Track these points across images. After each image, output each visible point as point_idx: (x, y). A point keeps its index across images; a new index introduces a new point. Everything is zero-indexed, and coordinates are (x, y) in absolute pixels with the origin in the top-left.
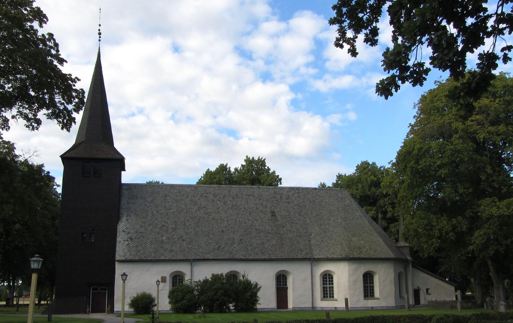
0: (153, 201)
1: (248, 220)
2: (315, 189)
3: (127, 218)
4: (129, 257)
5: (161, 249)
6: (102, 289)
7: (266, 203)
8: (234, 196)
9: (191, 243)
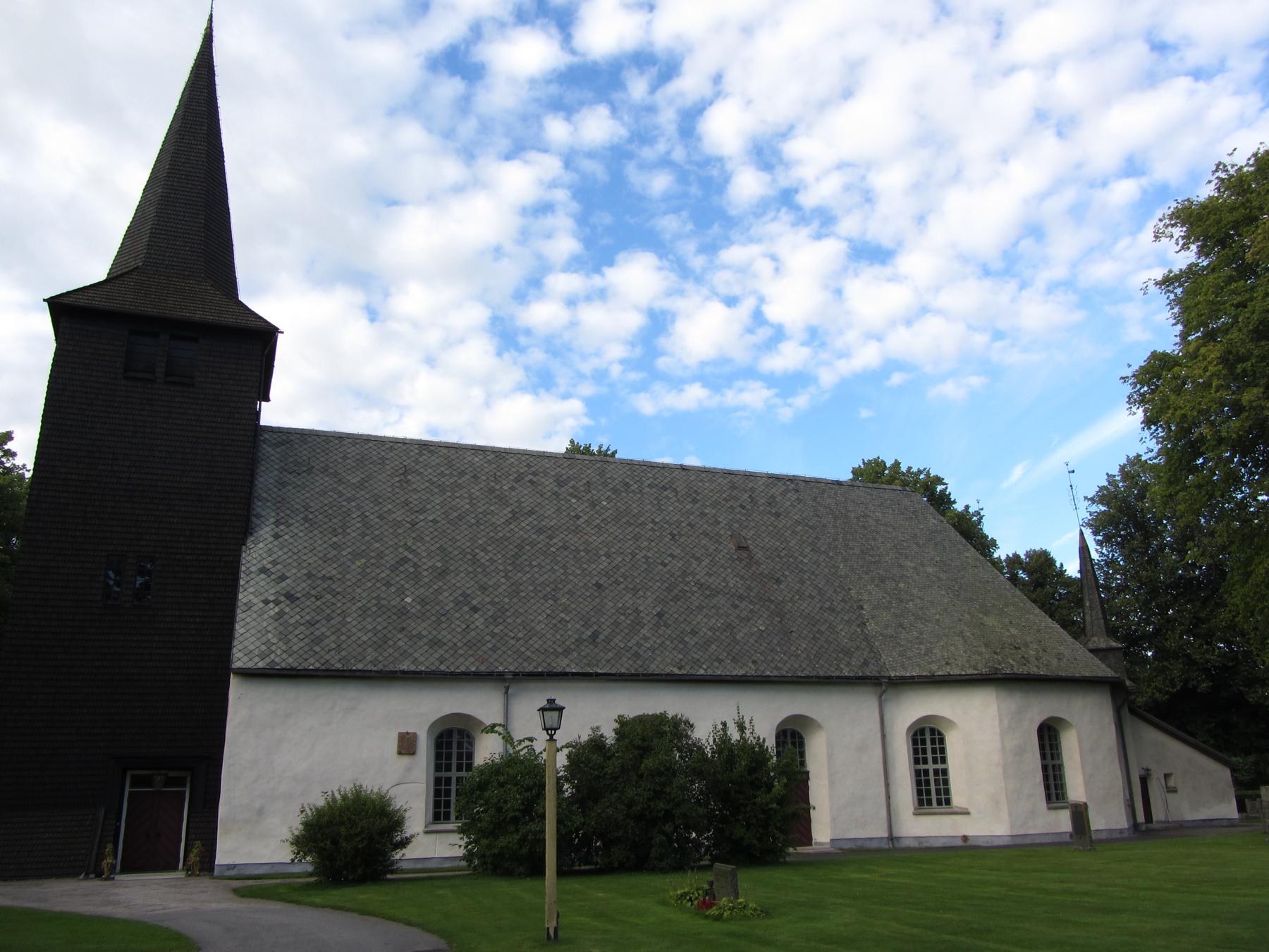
0: (366, 484)
1: (671, 555)
2: (838, 483)
3: (276, 530)
4: (283, 659)
5: (400, 636)
6: (169, 782)
7: (714, 511)
8: (618, 487)
9: (500, 620)
